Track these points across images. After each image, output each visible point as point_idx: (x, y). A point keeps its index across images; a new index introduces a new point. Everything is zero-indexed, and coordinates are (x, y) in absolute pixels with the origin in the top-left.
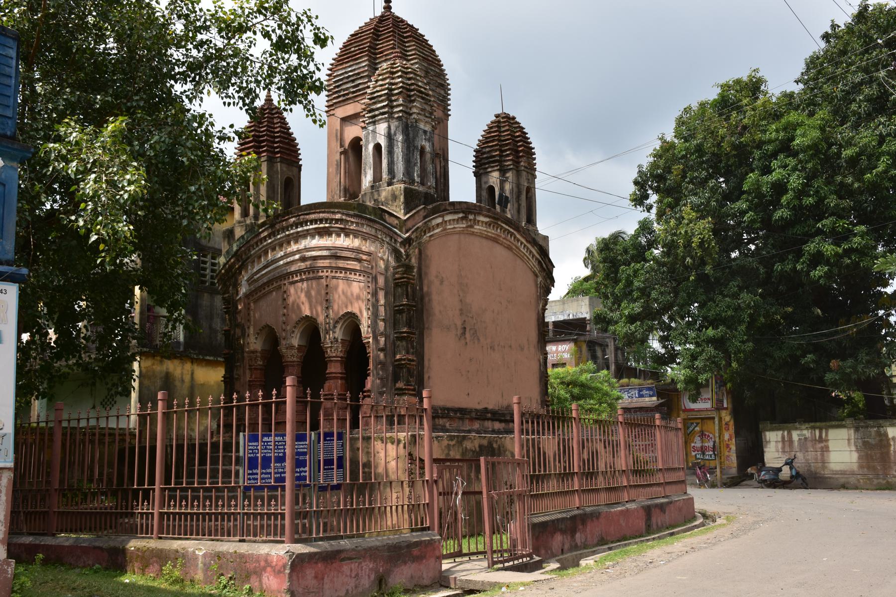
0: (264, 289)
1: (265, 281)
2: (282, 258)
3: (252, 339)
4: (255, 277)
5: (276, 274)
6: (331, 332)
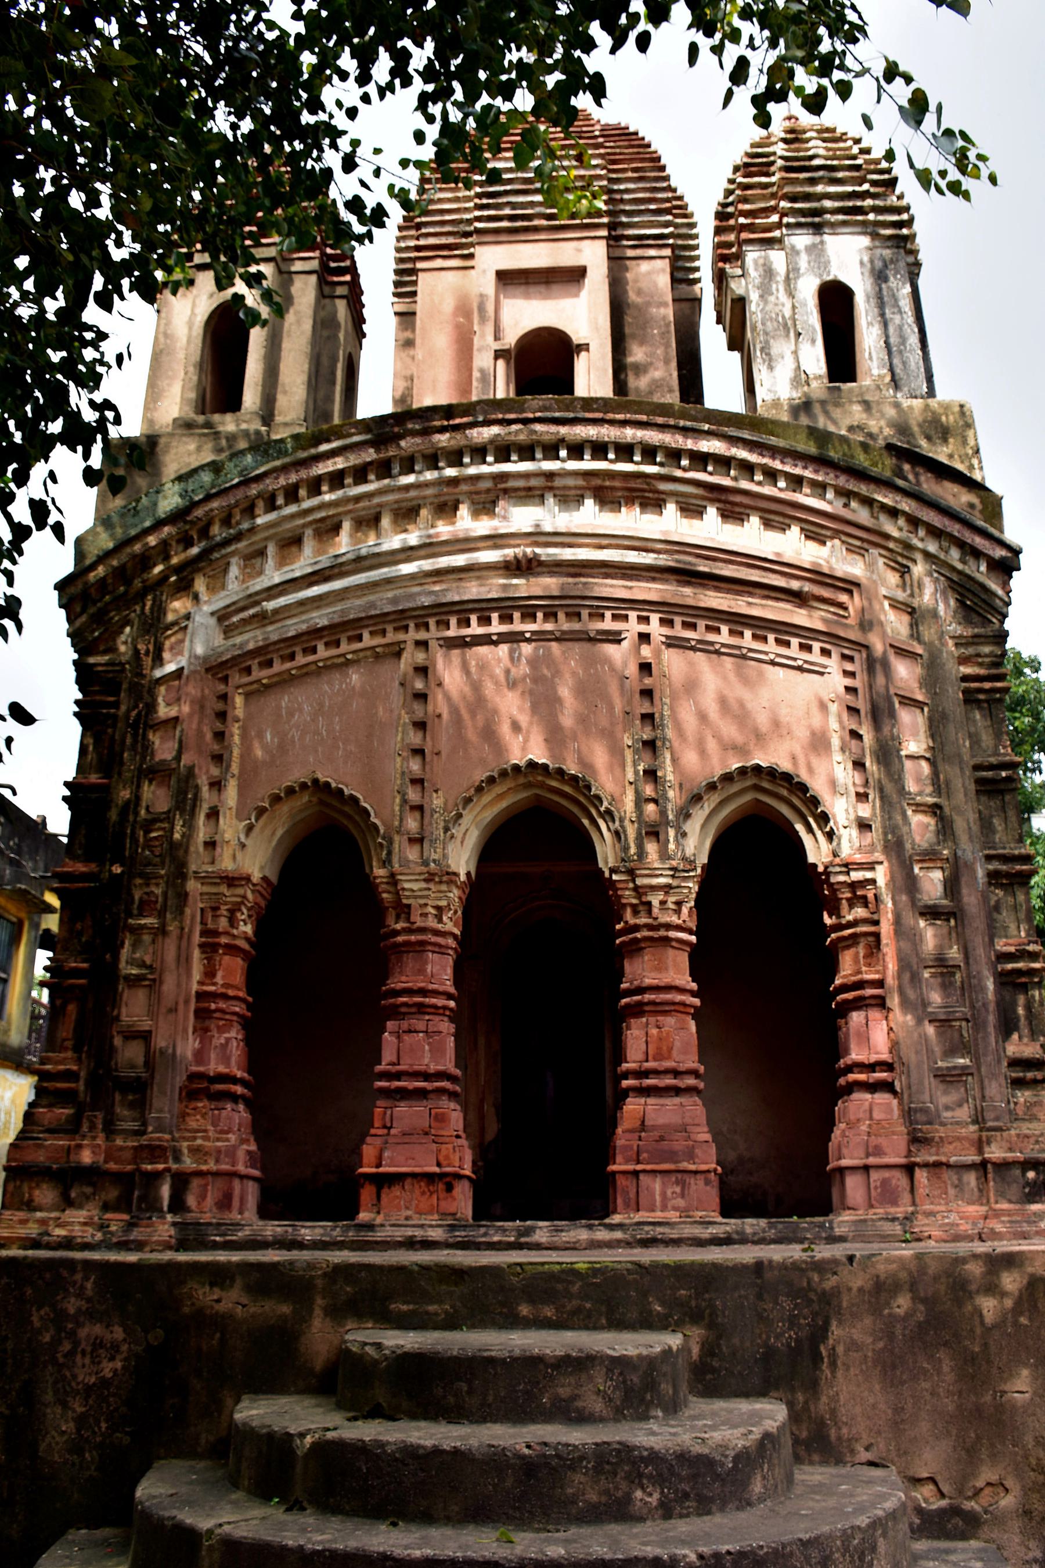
0: (292, 657)
1: (324, 622)
2: (408, 553)
3: (230, 828)
4: (270, 605)
5: (383, 601)
6: (672, 833)
